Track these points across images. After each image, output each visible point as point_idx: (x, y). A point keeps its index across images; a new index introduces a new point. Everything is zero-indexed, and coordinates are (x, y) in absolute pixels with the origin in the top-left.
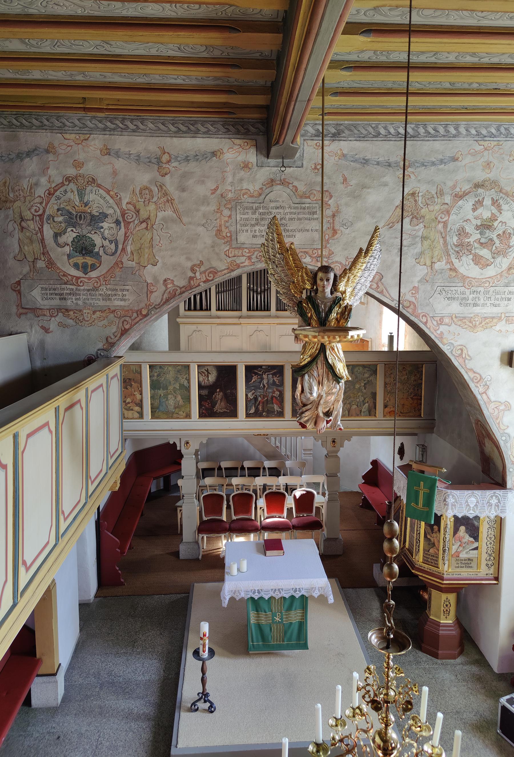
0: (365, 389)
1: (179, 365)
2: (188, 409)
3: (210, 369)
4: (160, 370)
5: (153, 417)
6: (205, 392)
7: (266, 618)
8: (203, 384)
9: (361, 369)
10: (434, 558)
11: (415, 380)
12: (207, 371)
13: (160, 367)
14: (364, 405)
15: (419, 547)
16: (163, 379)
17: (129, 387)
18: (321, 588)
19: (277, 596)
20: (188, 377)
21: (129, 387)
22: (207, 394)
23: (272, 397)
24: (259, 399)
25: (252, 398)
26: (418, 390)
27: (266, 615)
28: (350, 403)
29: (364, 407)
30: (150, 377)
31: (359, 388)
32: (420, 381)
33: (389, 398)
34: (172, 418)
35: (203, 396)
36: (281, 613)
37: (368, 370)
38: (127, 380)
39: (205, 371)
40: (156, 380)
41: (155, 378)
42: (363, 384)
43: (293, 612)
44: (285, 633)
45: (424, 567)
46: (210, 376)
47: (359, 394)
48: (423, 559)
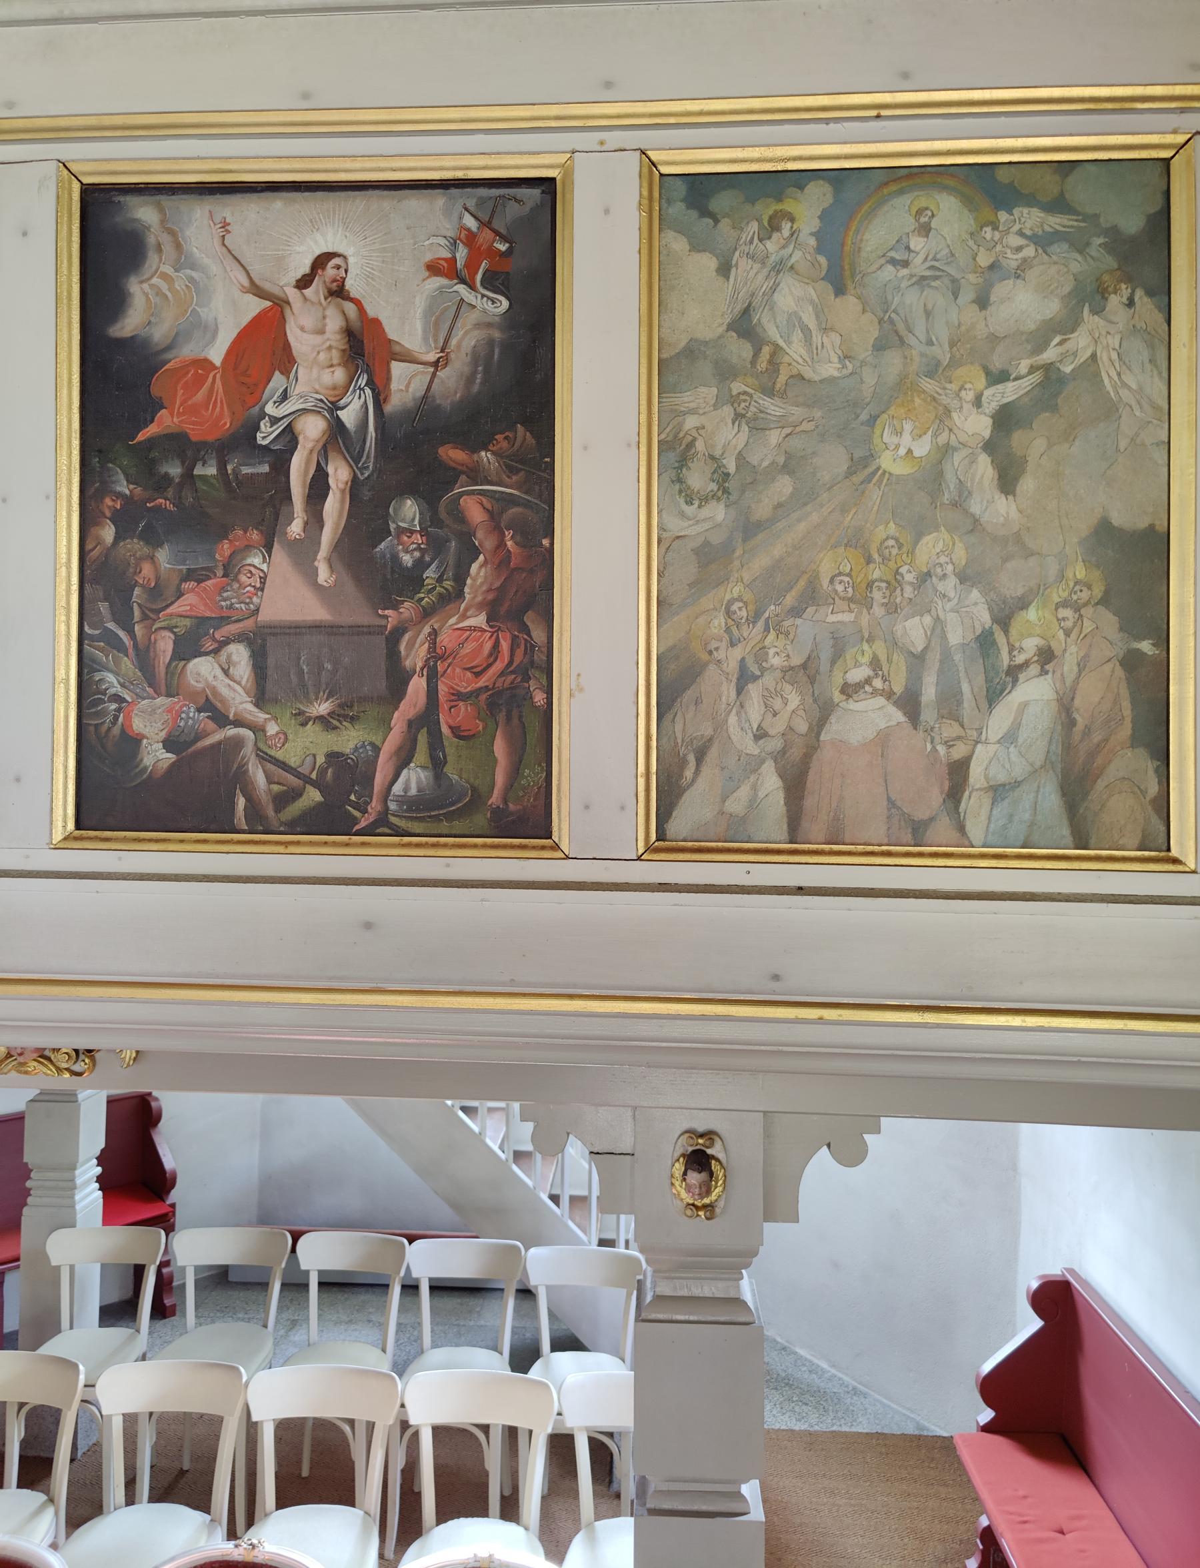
0: (1007, 482)
14: (993, 695)
29: (999, 721)
37: (1043, 241)
42: (978, 425)
47: (931, 547)
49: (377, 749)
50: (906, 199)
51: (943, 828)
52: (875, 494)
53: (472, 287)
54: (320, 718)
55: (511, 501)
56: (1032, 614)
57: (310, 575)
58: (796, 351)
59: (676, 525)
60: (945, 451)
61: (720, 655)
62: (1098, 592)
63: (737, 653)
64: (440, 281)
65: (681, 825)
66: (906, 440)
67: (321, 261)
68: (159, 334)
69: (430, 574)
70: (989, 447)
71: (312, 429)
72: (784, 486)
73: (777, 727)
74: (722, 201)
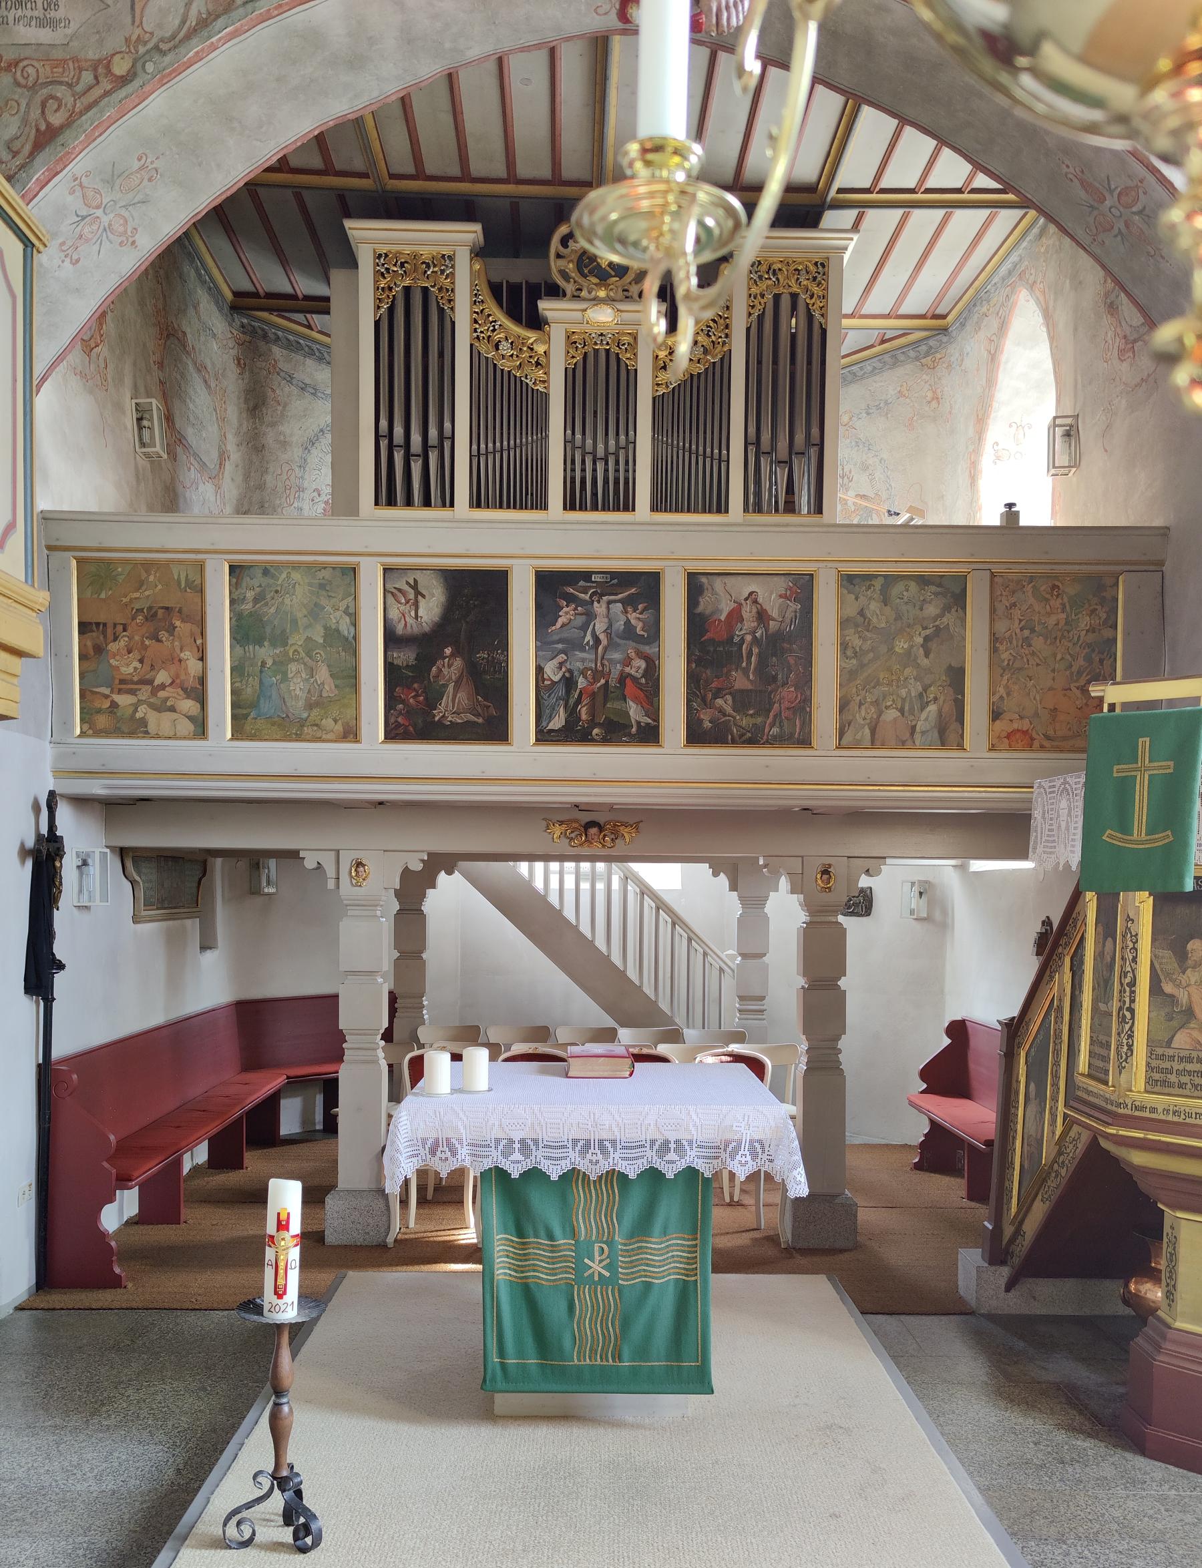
0: (927, 655)
1: (324, 567)
2: (350, 712)
3: (425, 581)
4: (265, 581)
5: (239, 732)
6: (406, 657)
7: (553, 1260)
8: (400, 629)
9: (913, 586)
10: (1189, 1067)
11: (1092, 630)
12: (415, 586)
13: (266, 572)
14: (922, 709)
15: (1131, 1037)
16: (272, 610)
17: (163, 635)
18: (760, 1142)
19: (594, 1166)
20: (352, 605)
21: (163, 635)
22: (412, 661)
23: (623, 678)
24: (582, 683)
25: (556, 678)
26: (1101, 661)
27: (554, 1249)
28: (876, 703)
29: (924, 715)
30: (232, 602)
31: (908, 652)
32: (1107, 633)
33: (1006, 687)
34: (299, 738)
35: (399, 667)
36: (610, 1242)
37: (936, 594)
38: (160, 612)
39: (406, 588)
40: (251, 614)
41: (247, 607)
42: (920, 640)
43: (655, 1243)
44: (626, 1324)
45: (1153, 1110)
46: (422, 603)
47: (908, 671)
48: (1149, 1081)
49: (766, 723)
50: (902, 583)
51: (909, 742)
52: (894, 658)
53: (791, 601)
54: (751, 715)
55: (800, 658)
56: (932, 688)
57: (748, 677)
58: (874, 620)
59: (844, 665)
60: (912, 647)
61: (854, 698)
62: (948, 683)
63: (859, 698)
64: (782, 600)
65: (847, 738)
66: (902, 644)
67: (751, 594)
68: (708, 612)
69: (780, 676)
70: (922, 646)
71: (749, 638)
72: (871, 655)
73: (868, 717)
74: (856, 581)
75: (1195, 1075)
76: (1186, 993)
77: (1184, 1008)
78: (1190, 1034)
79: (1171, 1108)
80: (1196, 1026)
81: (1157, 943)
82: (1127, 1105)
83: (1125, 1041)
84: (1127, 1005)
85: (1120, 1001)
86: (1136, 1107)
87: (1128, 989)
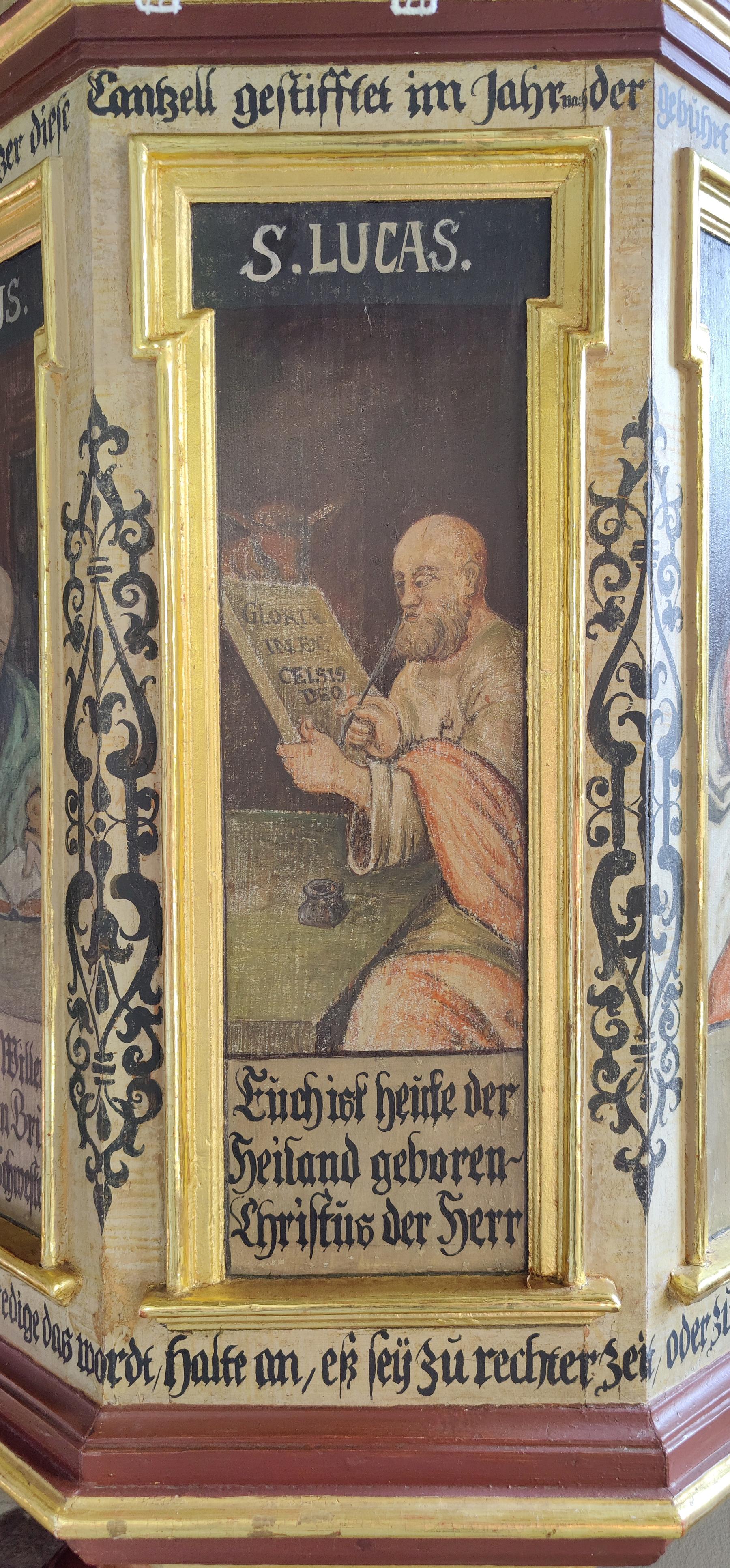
75: (464, 1169)
76: (401, 781)
77: (394, 857)
78: (429, 976)
79: (362, 1347)
80: (459, 940)
81: (248, 548)
82: (144, 1363)
83: (116, 1047)
84: (119, 865)
85: (74, 847)
86: (190, 1365)
87: (115, 786)
